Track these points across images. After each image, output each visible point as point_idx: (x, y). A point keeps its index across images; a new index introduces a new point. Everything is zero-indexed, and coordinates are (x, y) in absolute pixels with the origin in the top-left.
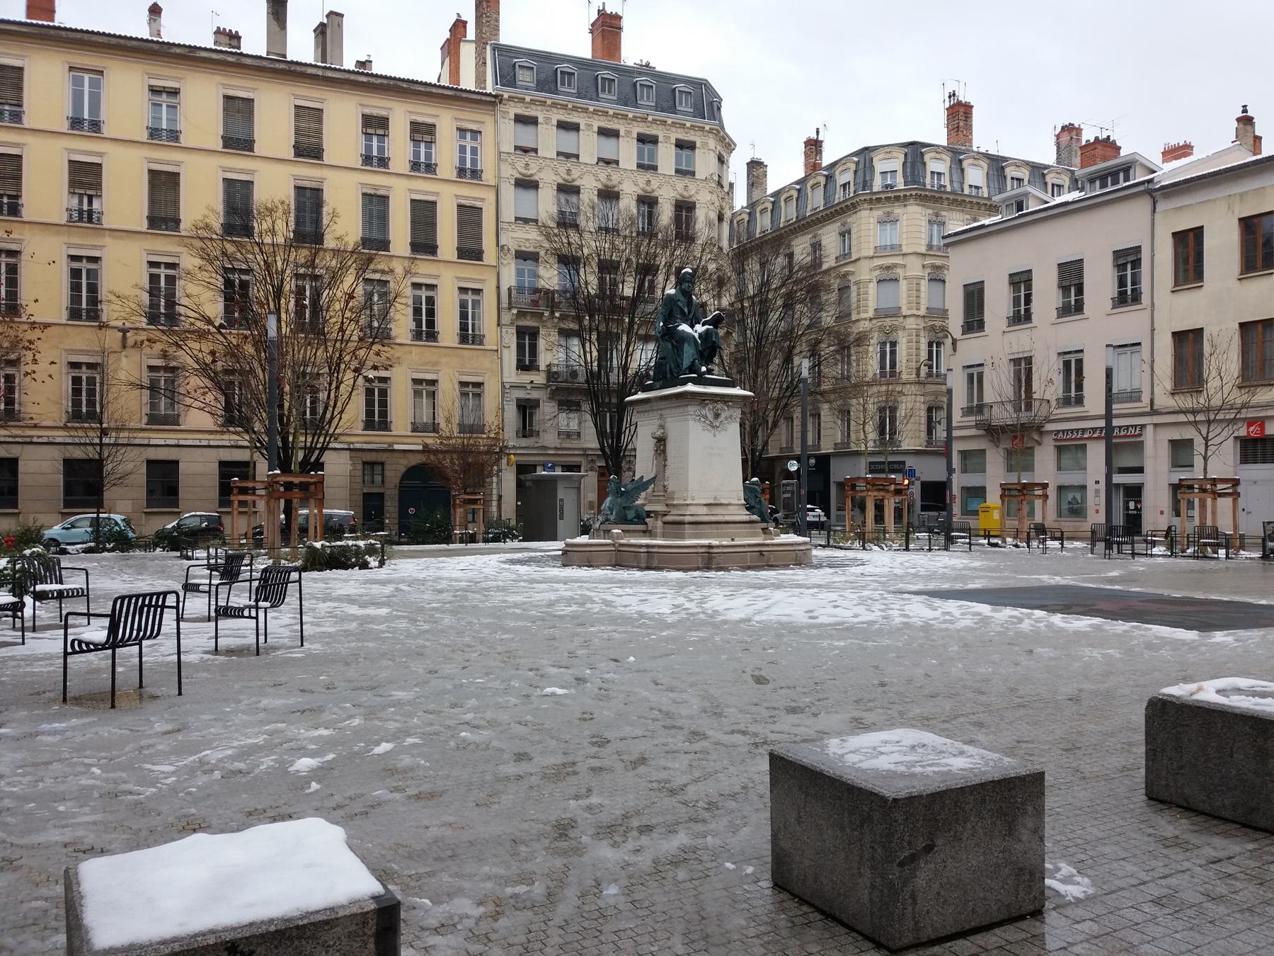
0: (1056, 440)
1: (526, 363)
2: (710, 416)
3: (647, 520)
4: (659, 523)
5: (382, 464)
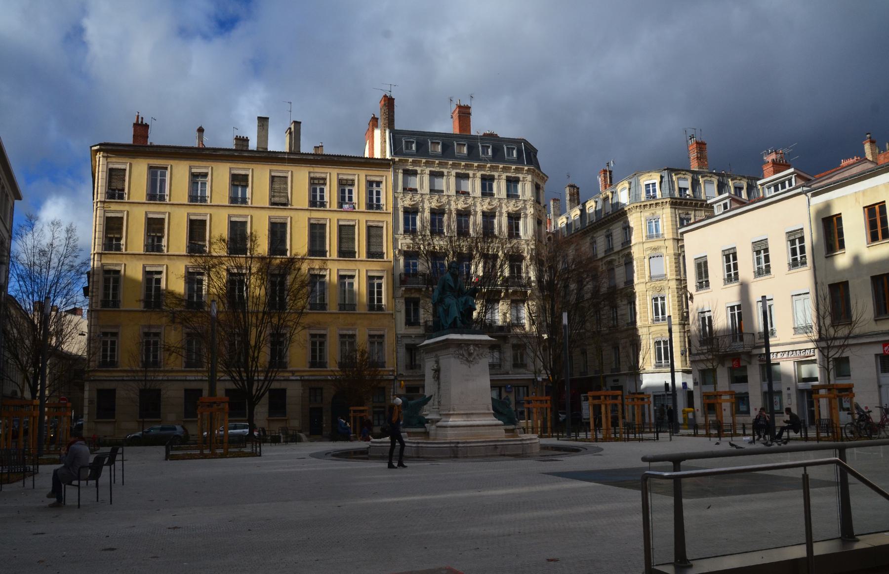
0: (760, 361)
1: (411, 321)
2: (466, 355)
5: (321, 389)
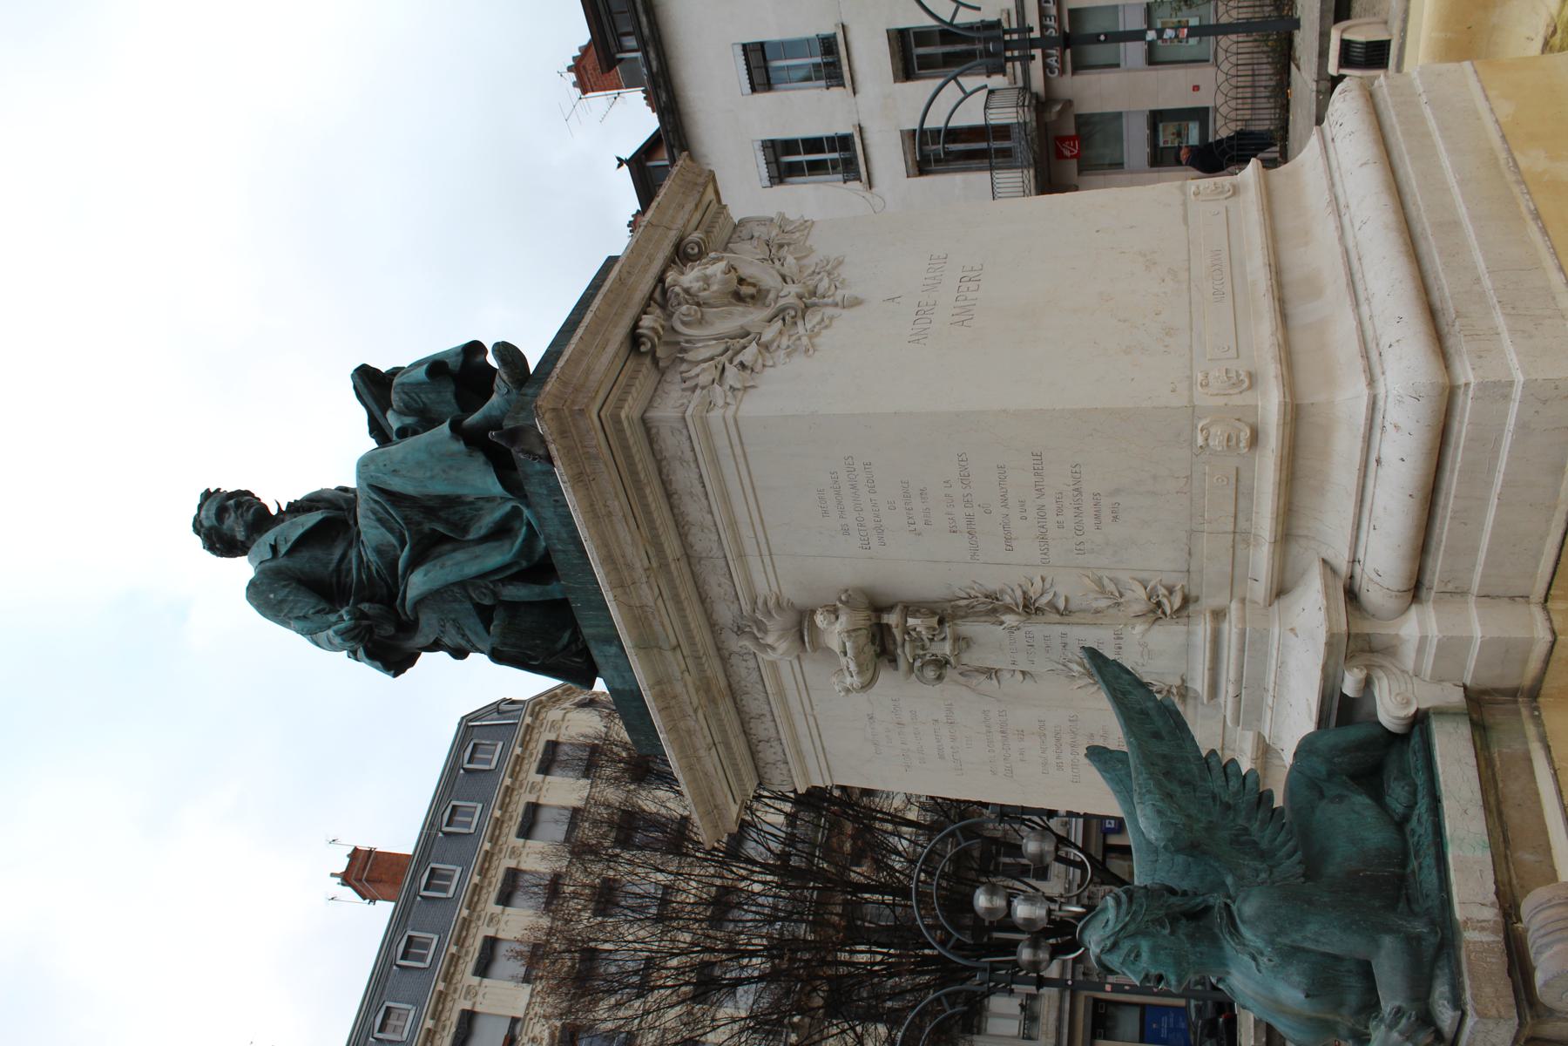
0: (1062, 72)
4: (1416, 629)
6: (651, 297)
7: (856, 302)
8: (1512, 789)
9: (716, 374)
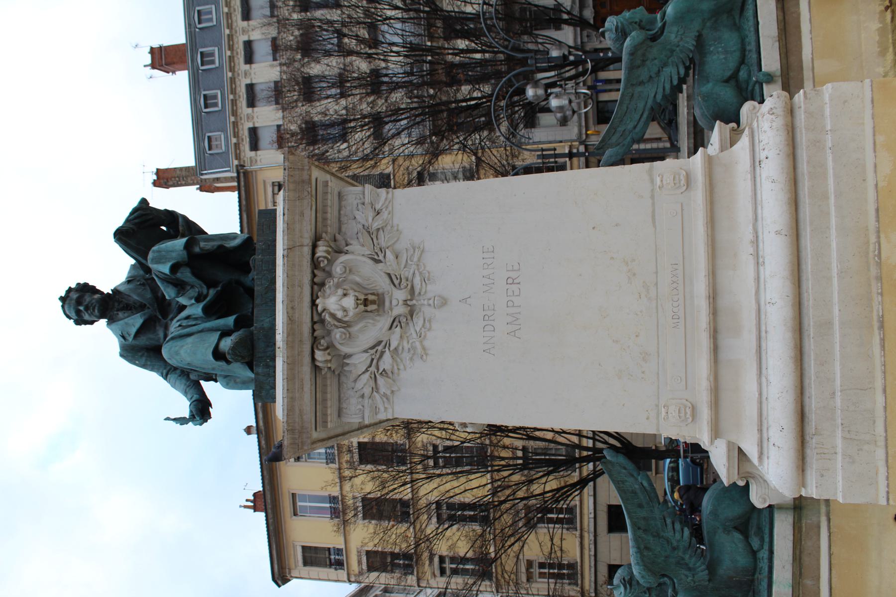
2: (373, 330)
3: (757, 499)
6: (314, 323)
7: (444, 302)
8: (808, 544)
9: (372, 383)
